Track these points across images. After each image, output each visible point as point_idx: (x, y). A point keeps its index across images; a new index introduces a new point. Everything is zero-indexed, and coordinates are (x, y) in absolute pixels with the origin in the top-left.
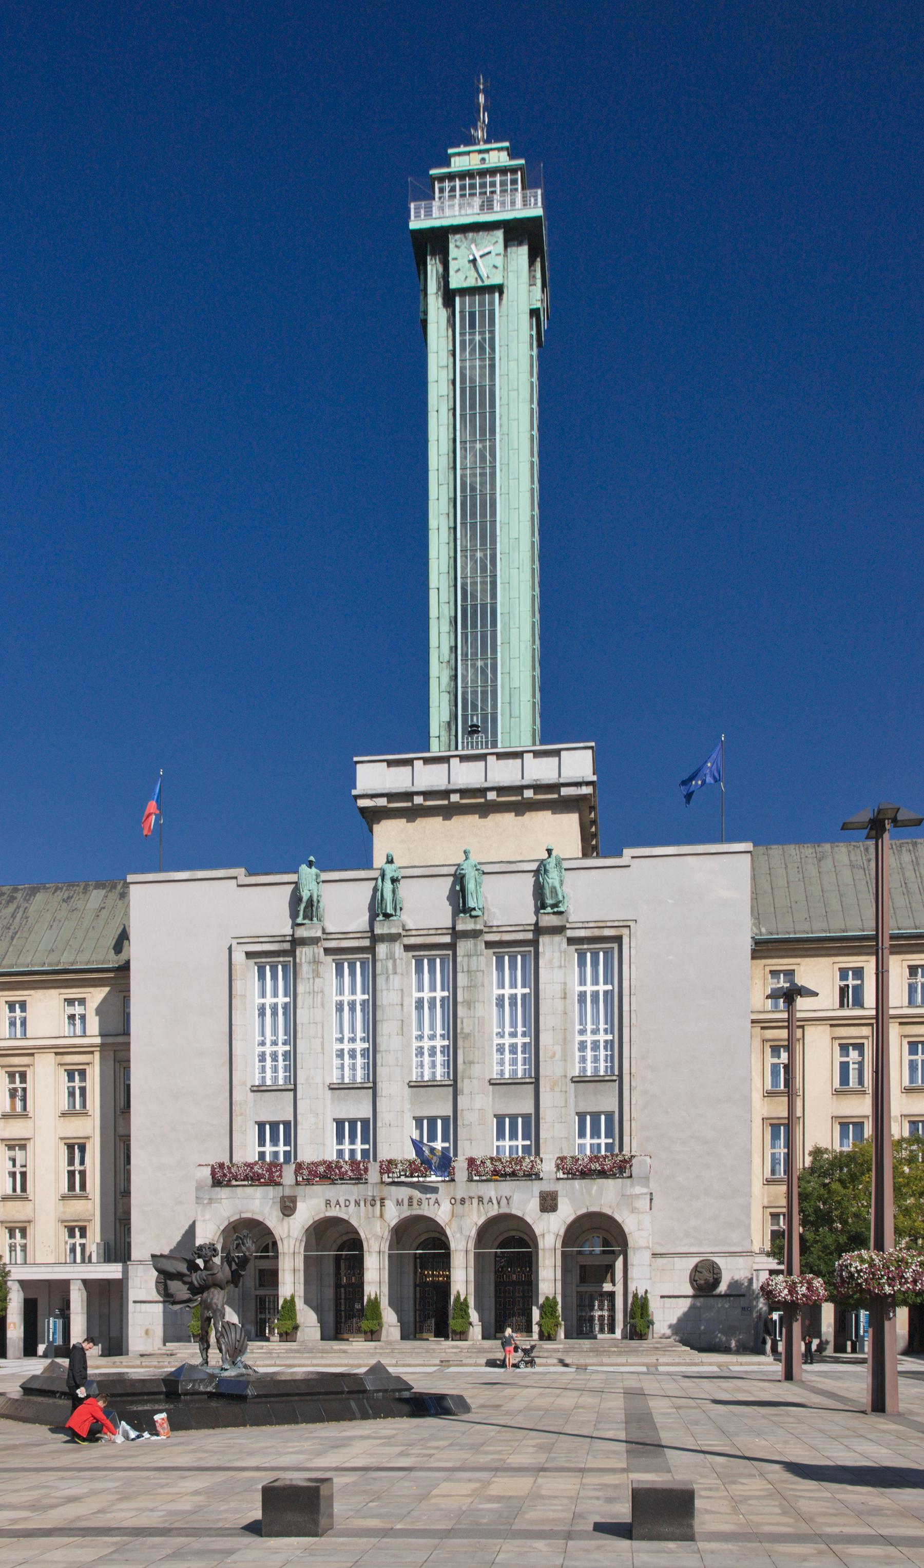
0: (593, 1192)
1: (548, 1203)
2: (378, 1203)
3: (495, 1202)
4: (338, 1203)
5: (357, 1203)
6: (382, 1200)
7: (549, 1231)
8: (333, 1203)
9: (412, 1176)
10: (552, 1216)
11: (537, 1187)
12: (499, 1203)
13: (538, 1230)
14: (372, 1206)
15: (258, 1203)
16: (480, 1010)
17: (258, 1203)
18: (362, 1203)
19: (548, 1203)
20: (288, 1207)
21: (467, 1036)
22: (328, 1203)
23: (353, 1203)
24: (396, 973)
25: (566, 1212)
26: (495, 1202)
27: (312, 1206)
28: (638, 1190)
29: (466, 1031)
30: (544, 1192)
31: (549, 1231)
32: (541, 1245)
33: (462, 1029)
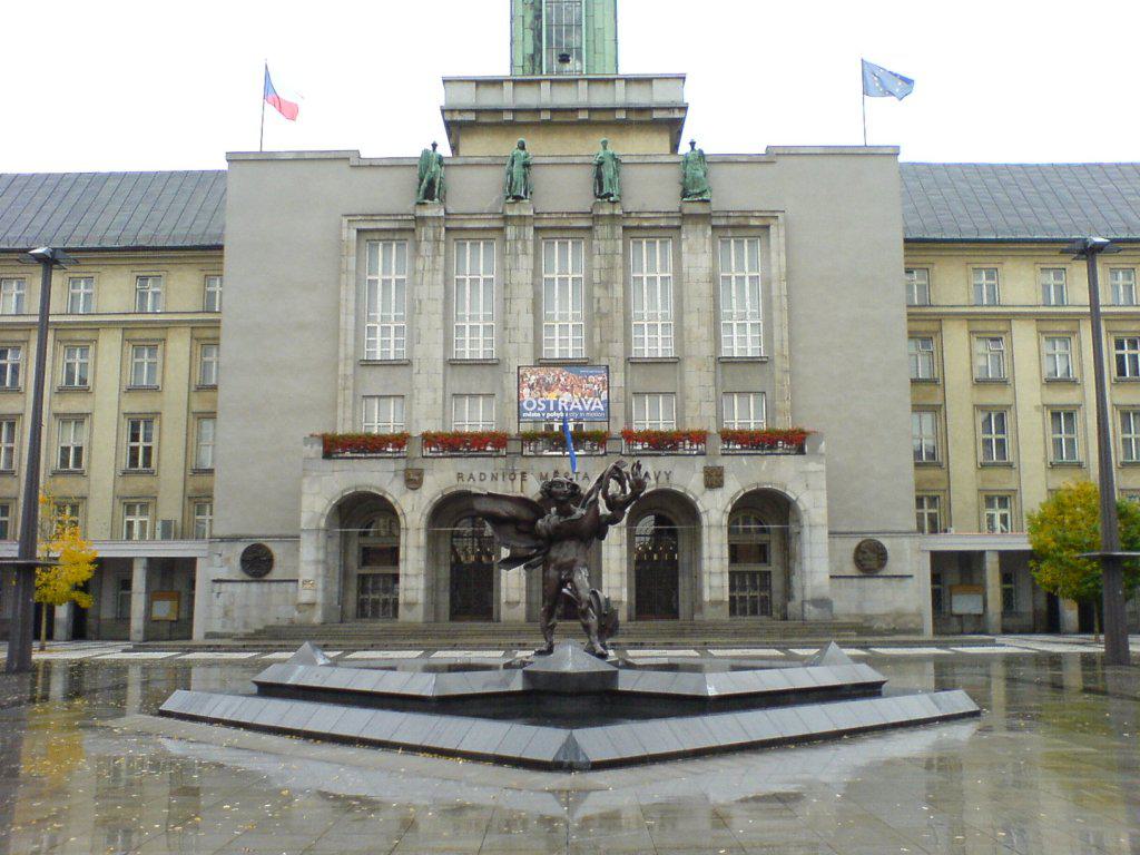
0: (763, 468)
1: (714, 479)
2: (519, 477)
3: (652, 477)
4: (471, 477)
5: (494, 478)
6: (523, 474)
7: (714, 508)
8: (466, 477)
9: (556, 450)
10: (718, 493)
11: (700, 463)
12: (657, 478)
13: (701, 508)
14: (512, 480)
15: (377, 476)
16: (619, 290)
17: (377, 476)
18: (500, 478)
19: (714, 479)
20: (413, 481)
21: (602, 316)
22: (460, 476)
23: (489, 479)
24: (526, 254)
25: (734, 487)
26: (652, 477)
27: (442, 477)
28: (813, 466)
29: (604, 310)
30: (709, 468)
31: (714, 508)
32: (705, 520)
33: (599, 308)
